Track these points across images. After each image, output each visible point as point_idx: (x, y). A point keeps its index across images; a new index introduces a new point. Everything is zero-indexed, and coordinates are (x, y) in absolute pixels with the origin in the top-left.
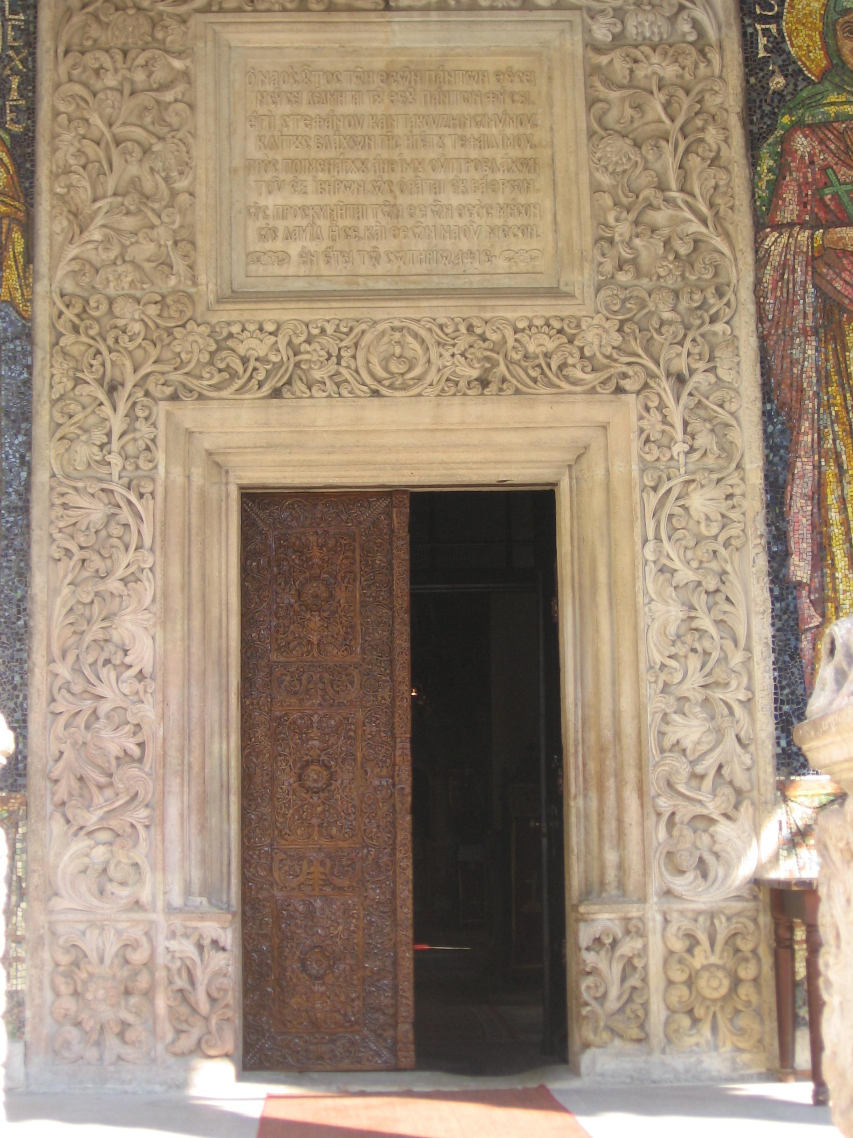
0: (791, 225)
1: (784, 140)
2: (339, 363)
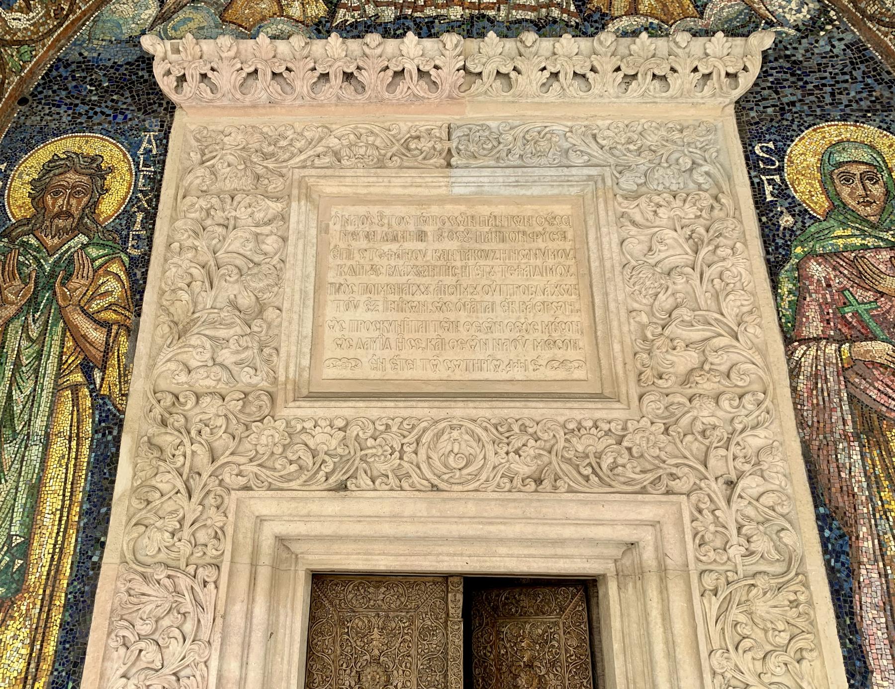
0: (817, 339)
2: (401, 458)
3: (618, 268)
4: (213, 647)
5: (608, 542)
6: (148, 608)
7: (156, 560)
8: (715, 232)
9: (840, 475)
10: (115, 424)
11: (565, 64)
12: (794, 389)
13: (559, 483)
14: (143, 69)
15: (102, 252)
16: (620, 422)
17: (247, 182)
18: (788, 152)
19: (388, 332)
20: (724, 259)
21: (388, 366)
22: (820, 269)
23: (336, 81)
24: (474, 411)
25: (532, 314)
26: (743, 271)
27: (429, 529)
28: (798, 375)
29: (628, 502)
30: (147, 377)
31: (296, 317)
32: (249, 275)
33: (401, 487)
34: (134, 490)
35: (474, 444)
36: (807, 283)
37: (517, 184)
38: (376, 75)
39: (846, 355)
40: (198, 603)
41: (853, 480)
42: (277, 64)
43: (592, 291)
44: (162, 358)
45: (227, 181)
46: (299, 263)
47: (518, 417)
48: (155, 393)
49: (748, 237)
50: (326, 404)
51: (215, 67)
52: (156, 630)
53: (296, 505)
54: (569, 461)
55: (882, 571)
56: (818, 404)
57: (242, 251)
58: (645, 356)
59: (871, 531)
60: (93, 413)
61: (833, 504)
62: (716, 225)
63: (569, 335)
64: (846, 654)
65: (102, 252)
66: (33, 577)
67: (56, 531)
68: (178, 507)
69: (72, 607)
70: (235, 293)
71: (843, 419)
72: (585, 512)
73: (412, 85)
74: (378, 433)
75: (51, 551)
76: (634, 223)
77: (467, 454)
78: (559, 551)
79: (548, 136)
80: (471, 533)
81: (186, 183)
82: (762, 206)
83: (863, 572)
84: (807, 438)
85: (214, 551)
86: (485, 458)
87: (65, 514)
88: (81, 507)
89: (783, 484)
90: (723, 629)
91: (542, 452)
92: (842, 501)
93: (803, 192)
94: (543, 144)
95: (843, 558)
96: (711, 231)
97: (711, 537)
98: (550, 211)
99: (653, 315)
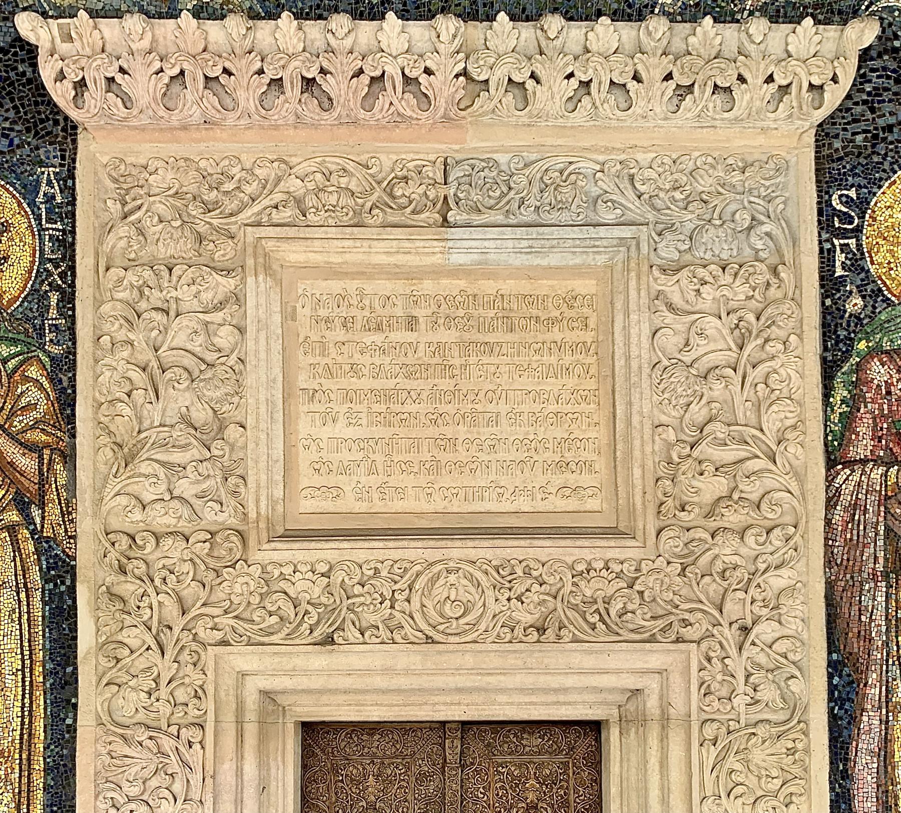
0: (864, 462)
1: (859, 368)
2: (392, 607)
3: (646, 370)
4: (206, 807)
5: (611, 690)
6: (134, 770)
7: (134, 721)
8: (767, 319)
9: (860, 618)
10: (67, 572)
11: (599, 68)
12: (828, 522)
13: (562, 633)
14: (23, 61)
15: (13, 350)
16: (634, 563)
17: (184, 247)
18: (872, 204)
19: (374, 452)
20: (773, 358)
21: (376, 496)
22: (882, 371)
23: (293, 91)
24: (473, 551)
25: (543, 429)
26: (793, 374)
27: (424, 682)
28: (836, 504)
29: (635, 651)
30: (95, 515)
31: (263, 436)
32: (202, 381)
33: (393, 639)
34: (101, 647)
35: (473, 590)
36: (865, 389)
37: (530, 251)
38: (346, 82)
39: (892, 480)
40: (185, 764)
41: (873, 624)
42: (211, 63)
43: (614, 399)
44: (109, 491)
45: (160, 244)
46: (263, 363)
47: (521, 558)
48: (107, 535)
49: (805, 328)
50: (306, 545)
51: (125, 66)
52: (144, 791)
53: (280, 659)
54: (575, 607)
55: (884, 718)
56: (851, 539)
57: (189, 347)
58: (668, 483)
59: (881, 677)
60: (39, 559)
61: (847, 650)
62: (770, 310)
63: (585, 455)
64: (833, 798)
65: (13, 350)
66: (6, 741)
67: (21, 693)
68: (150, 664)
69: (52, 771)
70: (187, 404)
71: (875, 556)
72: (589, 662)
73: (394, 98)
74: (365, 578)
75: (20, 714)
76: (670, 307)
77: (465, 601)
78: (562, 698)
79: (573, 177)
80: (469, 684)
81: (106, 248)
82: (829, 284)
83: (865, 719)
84: (833, 578)
86: (484, 605)
87: (28, 675)
88: (44, 667)
89: (800, 629)
90: (718, 777)
91: (546, 597)
92: (856, 646)
93: (879, 264)
94: (567, 192)
95: (847, 706)
96: (763, 319)
97: (717, 686)
98: (570, 288)
99: (682, 430)
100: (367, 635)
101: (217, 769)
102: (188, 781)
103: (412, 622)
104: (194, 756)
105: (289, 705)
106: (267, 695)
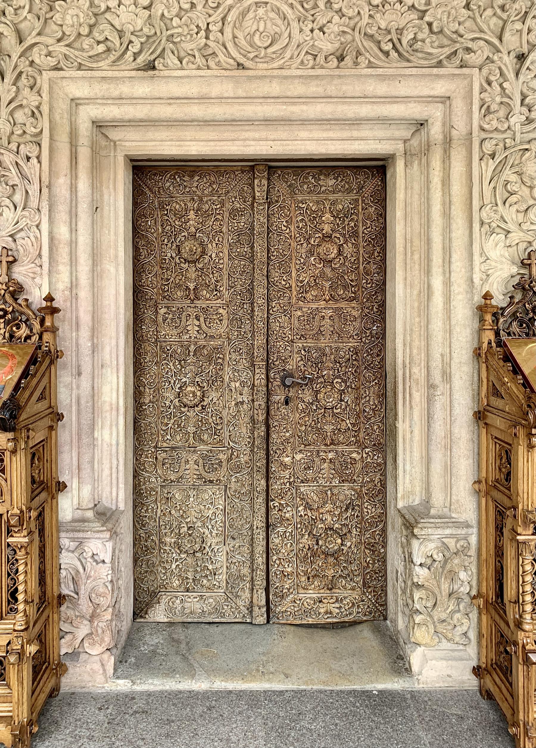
2: (207, 38)
85: (32, 129)
100: (184, 62)
101: (52, 181)
102: (27, 192)
103: (224, 50)
104: (32, 169)
105: (119, 140)
106: (99, 125)
